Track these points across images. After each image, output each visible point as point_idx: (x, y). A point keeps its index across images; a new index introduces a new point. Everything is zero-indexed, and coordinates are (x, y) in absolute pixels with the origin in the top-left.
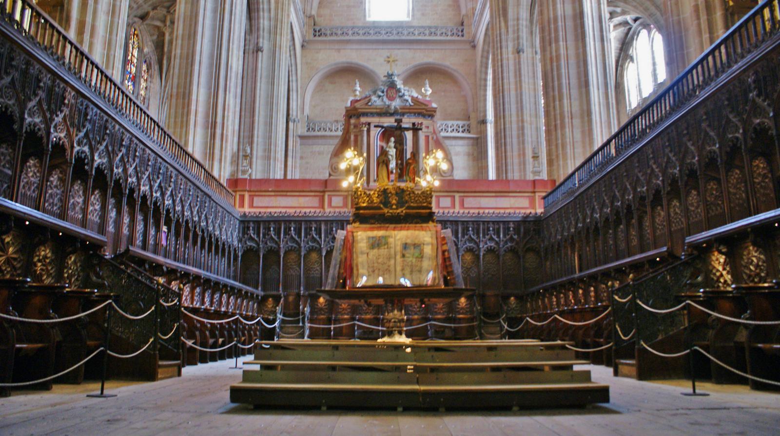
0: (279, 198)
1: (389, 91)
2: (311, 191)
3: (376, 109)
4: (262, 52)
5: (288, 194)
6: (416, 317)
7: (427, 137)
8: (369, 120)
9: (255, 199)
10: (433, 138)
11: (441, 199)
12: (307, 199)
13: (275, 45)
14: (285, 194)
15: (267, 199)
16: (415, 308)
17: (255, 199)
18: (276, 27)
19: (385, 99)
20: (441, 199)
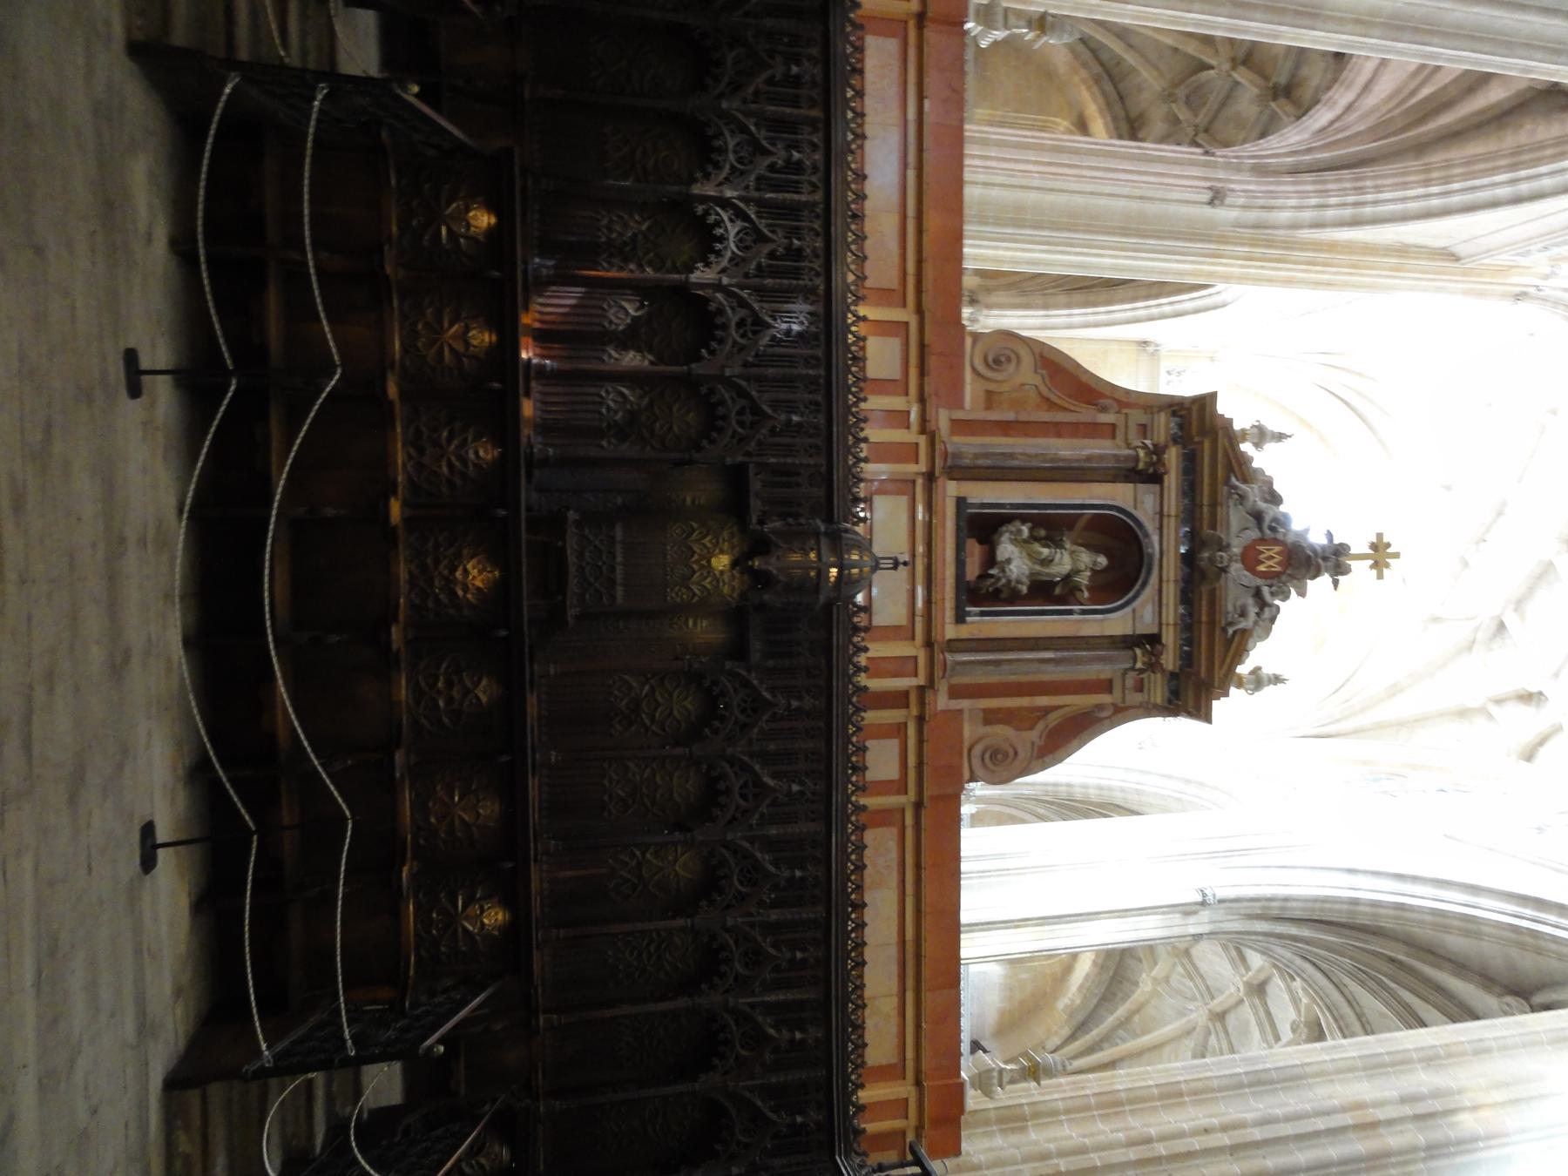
0: (894, 137)
1: (1277, 549)
2: (920, 262)
3: (1214, 505)
4: (1211, 203)
5: (911, 174)
6: (403, 692)
7: (1107, 686)
8: (1172, 480)
9: (892, 45)
10: (1101, 707)
11: (893, 745)
12: (893, 245)
13: (1223, 239)
14: (912, 159)
15: (893, 91)
16: (450, 685)
17: (892, 45)
18: (1270, 243)
19: (1254, 534)
20: (893, 745)
